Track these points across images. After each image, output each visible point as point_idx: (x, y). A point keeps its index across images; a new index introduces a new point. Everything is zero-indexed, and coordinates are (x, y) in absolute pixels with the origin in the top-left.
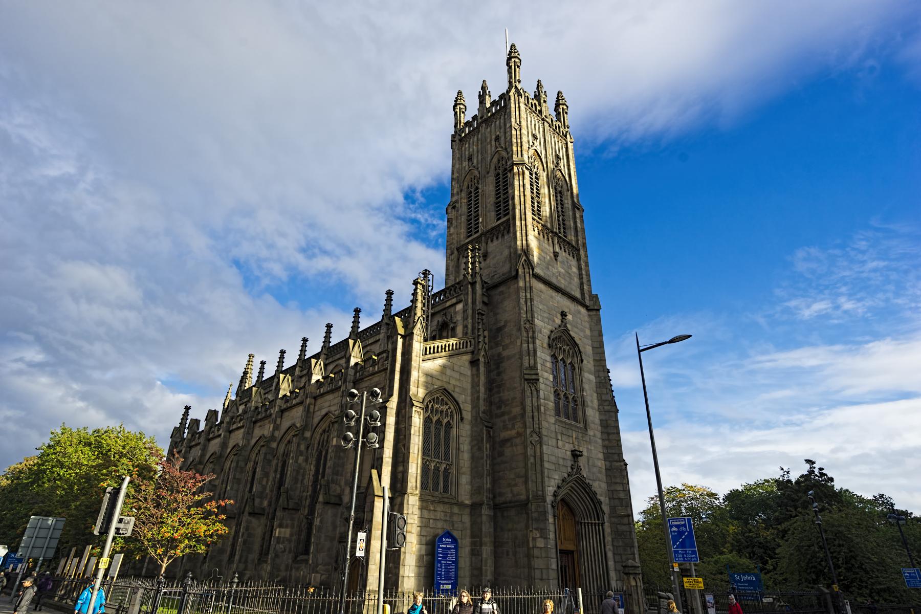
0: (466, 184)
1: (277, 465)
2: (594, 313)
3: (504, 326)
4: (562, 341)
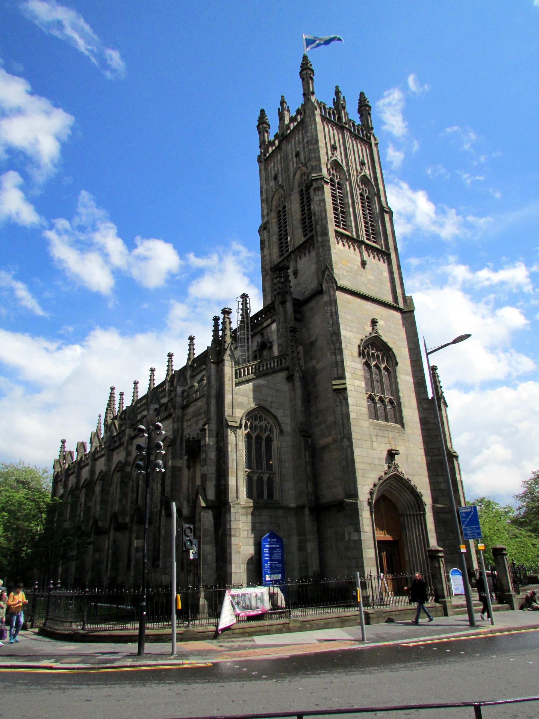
0: (274, 203)
1: (133, 487)
2: (408, 314)
3: (316, 340)
4: (376, 349)
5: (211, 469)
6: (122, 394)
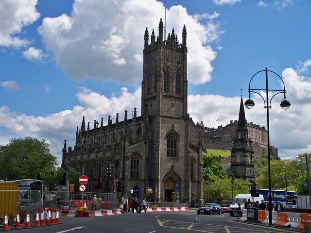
5: (121, 170)
6: (89, 123)
